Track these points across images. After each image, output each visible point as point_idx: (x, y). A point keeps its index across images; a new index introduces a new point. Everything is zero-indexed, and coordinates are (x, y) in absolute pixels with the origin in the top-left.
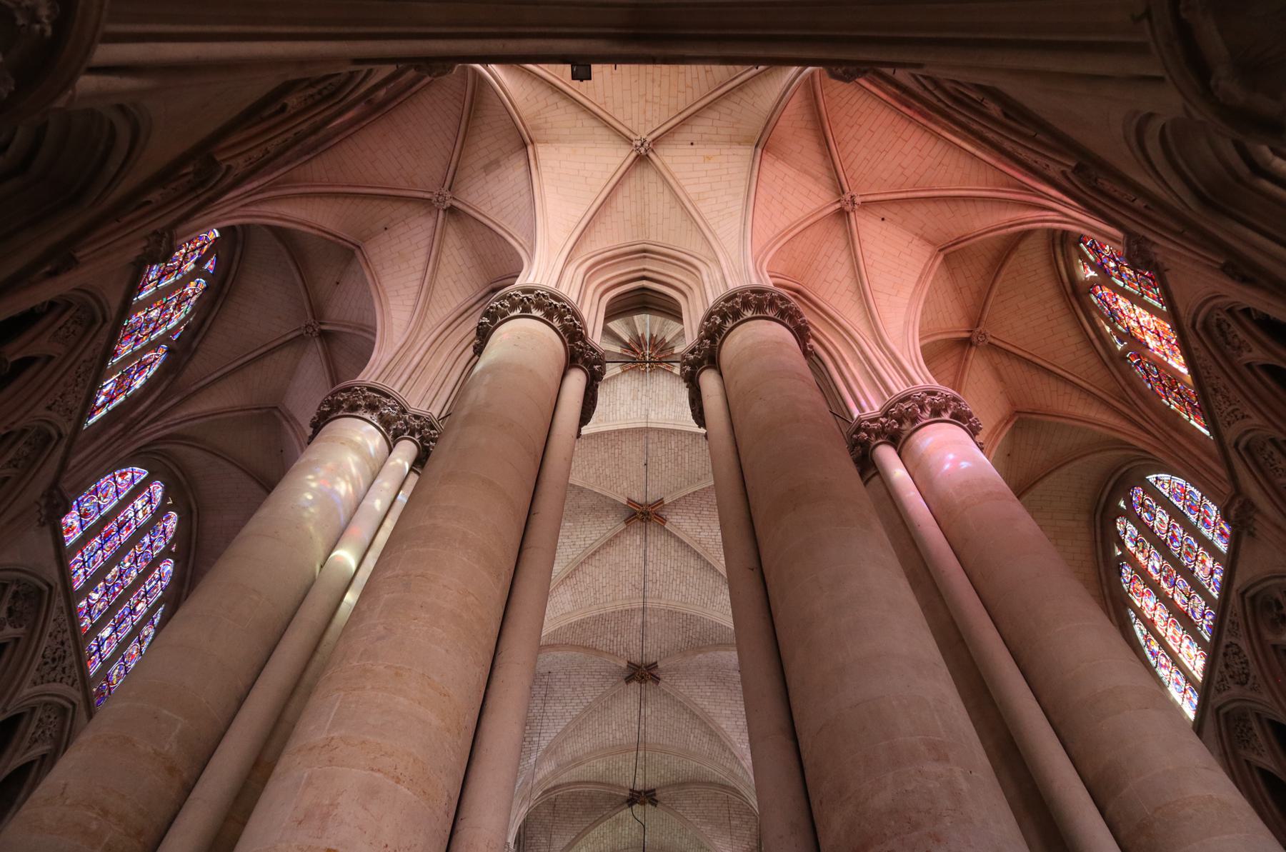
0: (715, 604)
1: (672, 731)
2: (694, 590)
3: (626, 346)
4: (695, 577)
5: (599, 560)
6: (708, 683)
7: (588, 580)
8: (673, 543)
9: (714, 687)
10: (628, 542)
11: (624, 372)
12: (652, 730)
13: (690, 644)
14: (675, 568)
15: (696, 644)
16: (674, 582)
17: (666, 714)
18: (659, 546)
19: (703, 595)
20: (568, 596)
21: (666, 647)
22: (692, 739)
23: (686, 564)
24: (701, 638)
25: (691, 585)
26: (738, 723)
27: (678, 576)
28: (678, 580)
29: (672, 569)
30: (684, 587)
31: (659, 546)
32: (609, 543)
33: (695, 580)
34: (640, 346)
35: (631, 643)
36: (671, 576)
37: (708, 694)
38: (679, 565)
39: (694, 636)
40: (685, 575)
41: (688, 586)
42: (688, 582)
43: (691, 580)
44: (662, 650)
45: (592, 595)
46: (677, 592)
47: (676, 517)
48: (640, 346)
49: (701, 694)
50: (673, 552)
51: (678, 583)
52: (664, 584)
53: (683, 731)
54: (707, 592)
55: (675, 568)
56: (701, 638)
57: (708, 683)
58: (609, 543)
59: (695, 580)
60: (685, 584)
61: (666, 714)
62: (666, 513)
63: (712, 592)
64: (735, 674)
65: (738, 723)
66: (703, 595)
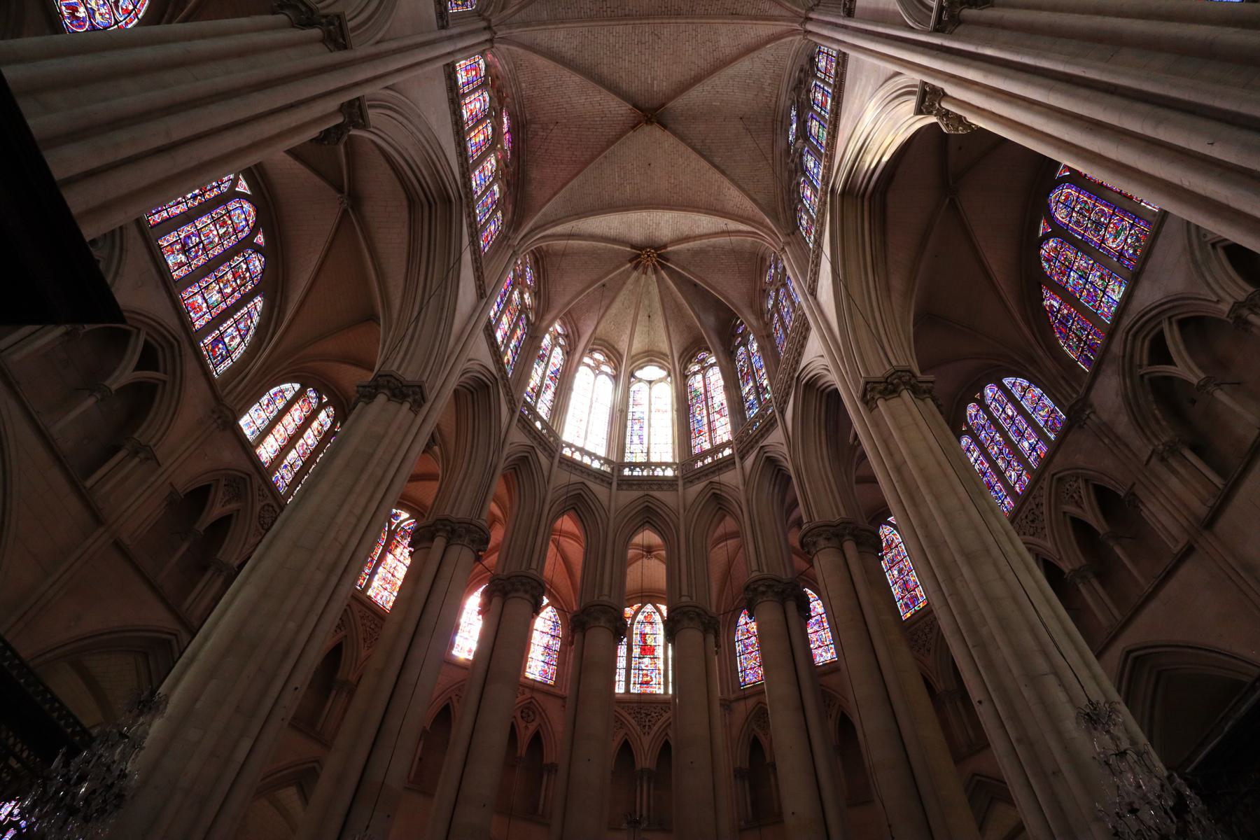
3: (663, 267)
5: (691, 70)
7: (702, 52)
8: (624, 86)
10: (665, 84)
11: (665, 246)
18: (636, 81)
20: (723, 41)
28: (617, 47)
31: (636, 81)
32: (684, 87)
34: (654, 265)
45: (699, 36)
47: (623, 112)
48: (654, 265)
50: (624, 77)
58: (684, 87)
62: (632, 115)
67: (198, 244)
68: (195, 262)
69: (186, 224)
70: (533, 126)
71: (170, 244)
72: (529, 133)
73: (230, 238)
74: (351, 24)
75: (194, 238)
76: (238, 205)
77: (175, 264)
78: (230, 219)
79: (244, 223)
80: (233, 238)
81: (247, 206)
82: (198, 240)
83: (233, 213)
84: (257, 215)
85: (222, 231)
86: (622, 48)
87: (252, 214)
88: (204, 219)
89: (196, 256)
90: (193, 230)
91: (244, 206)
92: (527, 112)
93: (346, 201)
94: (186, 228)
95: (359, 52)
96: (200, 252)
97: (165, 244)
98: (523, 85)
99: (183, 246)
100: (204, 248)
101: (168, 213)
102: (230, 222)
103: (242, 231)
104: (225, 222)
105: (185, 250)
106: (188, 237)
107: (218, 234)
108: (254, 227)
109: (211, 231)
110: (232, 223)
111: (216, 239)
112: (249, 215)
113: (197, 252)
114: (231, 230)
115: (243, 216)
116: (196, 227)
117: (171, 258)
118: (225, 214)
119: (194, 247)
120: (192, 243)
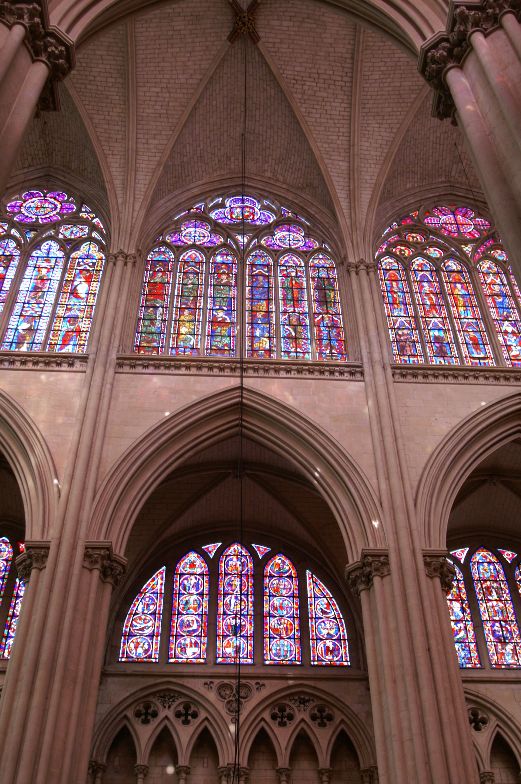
0: (366, 118)
1: (157, 60)
2: (376, 89)
4: (390, 89)
6: (225, 100)
9: (222, 108)
12: (153, 34)
13: (293, 82)
14: (398, 64)
15: (294, 90)
16: (382, 64)
17: (178, 50)
19: (372, 102)
21: (283, 50)
22: (153, 89)
23: (403, 76)
24: (305, 97)
25: (381, 85)
26: (188, 145)
27: (390, 68)
29: (398, 59)
30: (377, 77)
33: (387, 89)
35: (290, 5)
36: (389, 60)
37: (214, 103)
38: (402, 68)
39: (306, 88)
40: (391, 76)
41: (379, 81)
42: (384, 81)
43: (386, 85)
44: (277, 45)
46: (371, 69)
49: (214, 94)
51: (382, 69)
52: (380, 52)
53: (160, 76)
54: (376, 106)
55: (398, 64)
56: (305, 97)
57: (225, 100)
59: (387, 89)
60: (382, 76)
61: (178, 50)
63: (377, 113)
64: (238, 129)
65: (188, 145)
66: (372, 102)
67: (501, 626)
68: (515, 636)
69: (483, 629)
70: (453, 173)
71: (497, 653)
72: (459, 179)
73: (502, 589)
74: (372, 546)
75: (496, 628)
76: (476, 567)
77: (513, 657)
78: (485, 581)
79: (492, 567)
80: (502, 586)
81: (478, 557)
82: (497, 624)
83: (481, 576)
84: (488, 550)
85: (495, 596)
86: (386, 62)
87: (485, 553)
88: (482, 609)
89: (511, 633)
90: (489, 625)
91: (477, 559)
92: (437, 181)
93: (494, 481)
94: (486, 632)
95: (392, 545)
96: (508, 626)
97: (495, 658)
98: (408, 186)
99: (500, 642)
100: (505, 621)
101: (471, 643)
102: (488, 583)
103: (498, 572)
104: (488, 588)
105: (503, 641)
106: (494, 632)
107: (496, 600)
108: (498, 559)
109: (493, 607)
110: (490, 581)
111: (501, 605)
112: (485, 557)
113: (507, 630)
114: (495, 585)
115: (486, 564)
116: (487, 620)
117: (507, 658)
118: (482, 584)
119: (503, 631)
120: (499, 632)
